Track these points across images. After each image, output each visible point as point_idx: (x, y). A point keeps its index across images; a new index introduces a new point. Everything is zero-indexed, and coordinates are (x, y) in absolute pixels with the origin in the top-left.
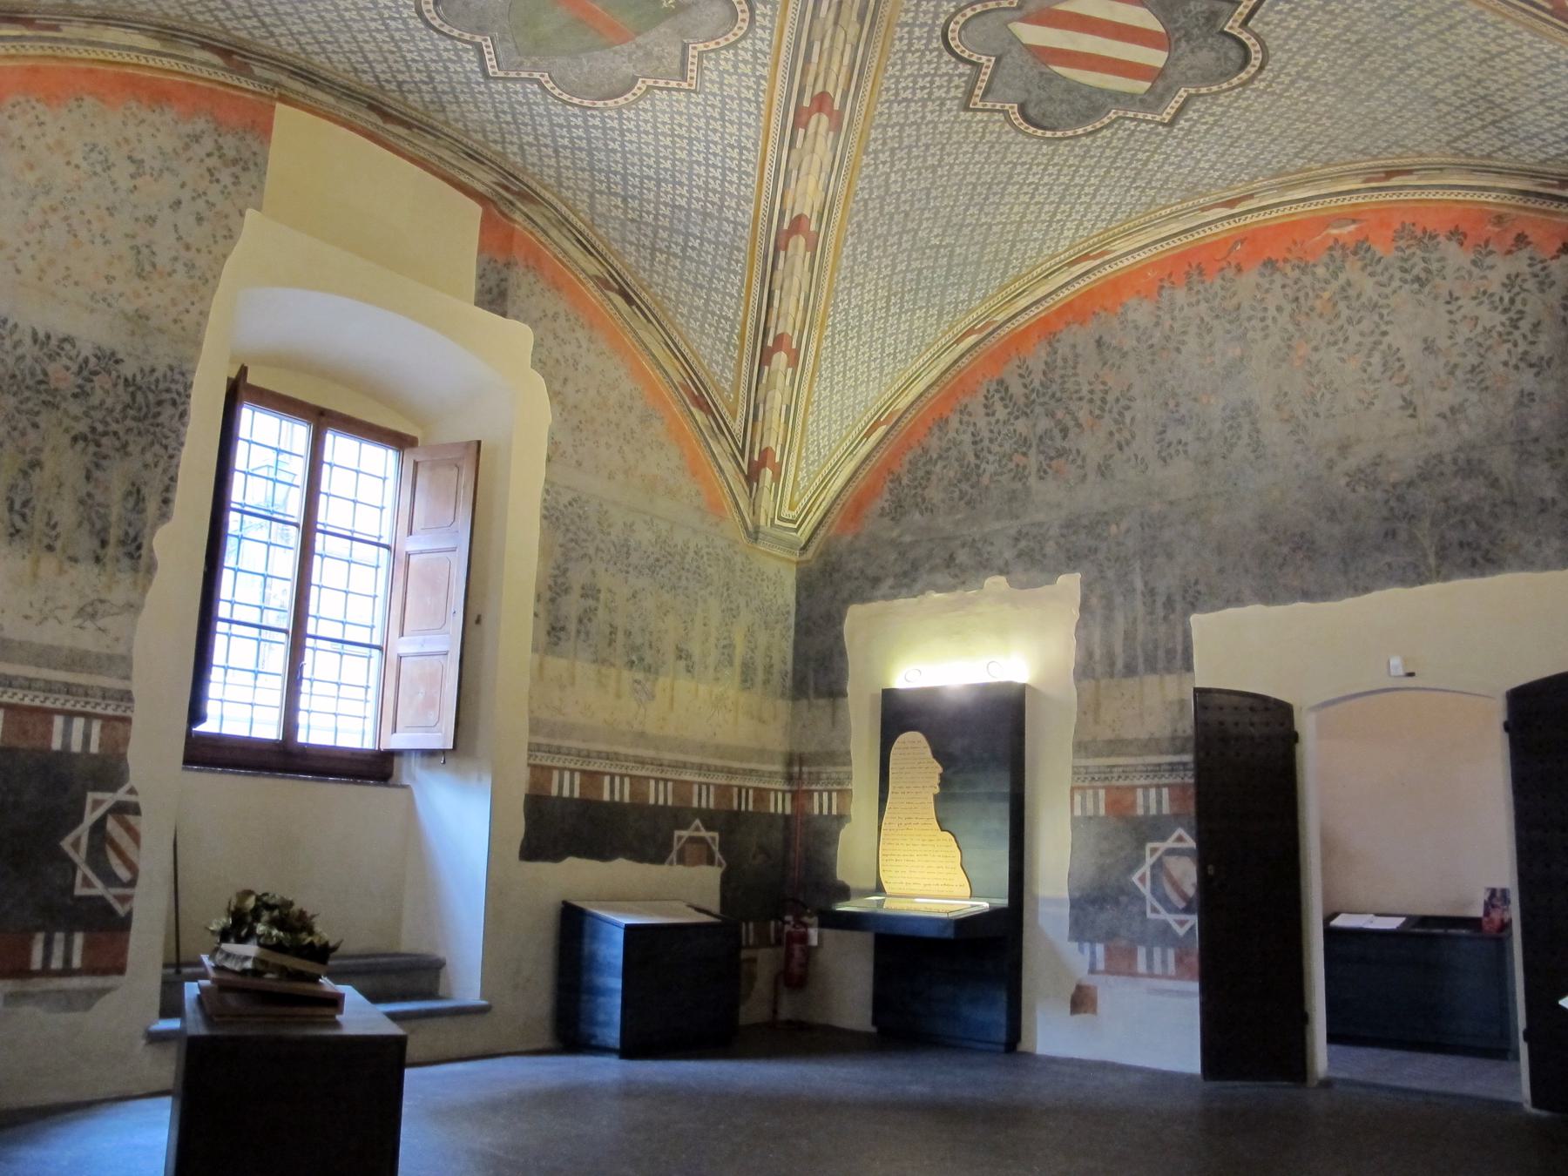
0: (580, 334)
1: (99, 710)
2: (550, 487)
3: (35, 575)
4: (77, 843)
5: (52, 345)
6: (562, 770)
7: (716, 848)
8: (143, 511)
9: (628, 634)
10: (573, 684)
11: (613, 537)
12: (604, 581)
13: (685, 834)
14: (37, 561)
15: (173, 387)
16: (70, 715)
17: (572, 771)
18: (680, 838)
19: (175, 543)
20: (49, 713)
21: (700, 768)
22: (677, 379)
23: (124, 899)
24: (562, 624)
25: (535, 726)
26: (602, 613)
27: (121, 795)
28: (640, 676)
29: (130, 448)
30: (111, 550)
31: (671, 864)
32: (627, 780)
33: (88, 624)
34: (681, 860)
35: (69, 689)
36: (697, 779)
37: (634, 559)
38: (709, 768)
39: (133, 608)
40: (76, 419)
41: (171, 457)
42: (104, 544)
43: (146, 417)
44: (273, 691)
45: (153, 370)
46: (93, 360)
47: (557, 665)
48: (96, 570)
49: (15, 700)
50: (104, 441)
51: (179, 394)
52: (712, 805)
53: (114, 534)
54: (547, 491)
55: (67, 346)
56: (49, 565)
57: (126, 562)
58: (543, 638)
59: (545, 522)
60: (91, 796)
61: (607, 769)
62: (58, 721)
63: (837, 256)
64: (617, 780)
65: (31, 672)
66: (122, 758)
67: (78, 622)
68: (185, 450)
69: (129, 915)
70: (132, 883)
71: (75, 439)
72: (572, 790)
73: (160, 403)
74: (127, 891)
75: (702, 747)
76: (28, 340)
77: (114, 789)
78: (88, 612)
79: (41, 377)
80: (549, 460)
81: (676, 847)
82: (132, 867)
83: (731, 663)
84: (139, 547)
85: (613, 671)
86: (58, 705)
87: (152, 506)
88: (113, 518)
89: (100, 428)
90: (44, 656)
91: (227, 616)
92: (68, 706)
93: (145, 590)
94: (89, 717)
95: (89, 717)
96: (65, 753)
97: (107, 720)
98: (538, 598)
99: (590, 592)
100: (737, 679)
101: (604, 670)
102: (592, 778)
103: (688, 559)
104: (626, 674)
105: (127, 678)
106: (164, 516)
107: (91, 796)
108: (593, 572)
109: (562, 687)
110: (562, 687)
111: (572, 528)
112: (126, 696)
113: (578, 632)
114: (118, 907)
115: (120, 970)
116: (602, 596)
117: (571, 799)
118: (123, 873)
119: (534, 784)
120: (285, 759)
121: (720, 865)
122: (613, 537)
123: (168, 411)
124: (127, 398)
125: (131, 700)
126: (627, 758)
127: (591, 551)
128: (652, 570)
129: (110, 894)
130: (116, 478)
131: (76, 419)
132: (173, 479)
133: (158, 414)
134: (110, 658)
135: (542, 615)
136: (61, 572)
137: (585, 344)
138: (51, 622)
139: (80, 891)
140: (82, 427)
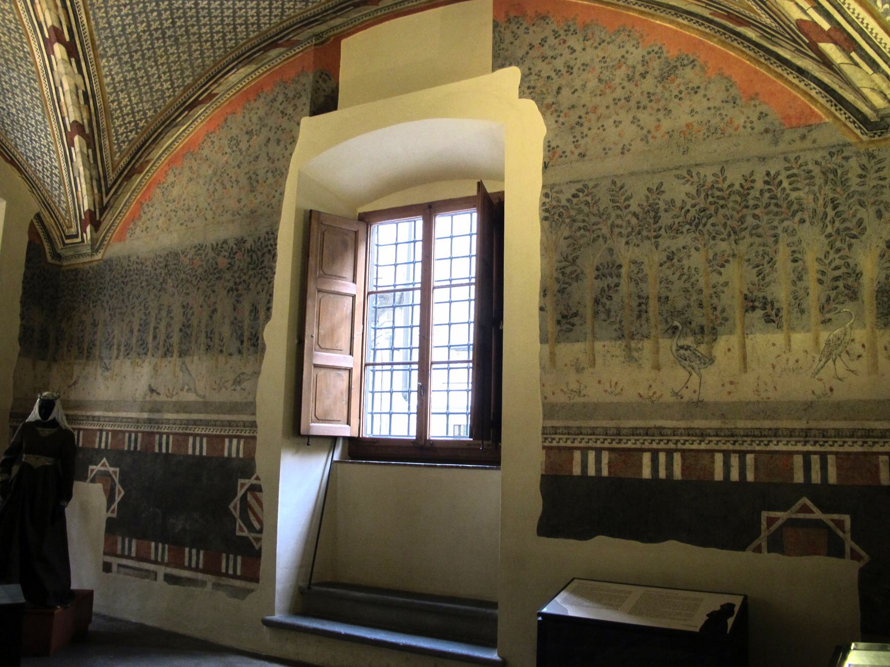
0: (572, 41)
1: (243, 434)
2: (549, 190)
3: (217, 367)
4: (235, 506)
5: (217, 248)
6: (584, 451)
7: (847, 537)
8: (258, 318)
9: (663, 300)
10: (593, 363)
11: (634, 208)
12: (625, 254)
13: (782, 516)
14: (217, 359)
15: (269, 243)
16: (231, 437)
17: (599, 451)
18: (771, 521)
19: (276, 332)
20: (222, 437)
21: (806, 435)
22: (706, 13)
23: (258, 540)
24: (574, 310)
25: (550, 410)
26: (625, 288)
27: (253, 481)
28: (689, 341)
29: (252, 286)
30: (245, 344)
31: (758, 549)
32: (677, 457)
33: (238, 388)
34: (776, 545)
35: (230, 424)
36: (800, 447)
37: (666, 219)
38: (824, 433)
39: (257, 374)
40: (228, 281)
41: (270, 283)
42: (242, 342)
43: (257, 266)
44: (408, 405)
45: (260, 238)
46: (235, 247)
47: (570, 351)
48: (239, 357)
49: (210, 433)
50: (240, 287)
51: (271, 245)
52: (832, 478)
53: (246, 334)
54: (546, 195)
55: (225, 245)
56: (222, 359)
57: (252, 349)
58: (551, 327)
59: (546, 223)
60: (241, 481)
61: (647, 445)
62: (227, 441)
64: (662, 457)
65: (214, 417)
66: (253, 459)
67: (233, 387)
68: (276, 276)
69: (260, 548)
70: (261, 531)
71: (228, 291)
72: (599, 469)
73: (263, 255)
74: (258, 535)
75: (809, 406)
76: (210, 251)
77: (249, 478)
78: (237, 382)
79: (215, 266)
80: (546, 166)
81: (765, 532)
82: (260, 522)
83: (853, 295)
84: (257, 340)
85: (647, 345)
86: (226, 433)
87: (262, 314)
88: (246, 327)
89: (238, 280)
90: (221, 408)
91: (371, 361)
92: (230, 433)
93: (261, 363)
94: (239, 437)
95: (239, 437)
96: (229, 458)
97: (246, 438)
98: (544, 293)
99: (609, 270)
100: (870, 316)
101: (633, 344)
102: (631, 456)
103: (754, 193)
104: (667, 344)
105: (254, 414)
106: (268, 318)
107: (241, 481)
108: (611, 250)
109: (579, 370)
110: (579, 370)
111: (580, 217)
112: (253, 425)
113: (596, 313)
114: (255, 544)
115: (257, 580)
116: (623, 271)
117: (599, 477)
118: (257, 525)
119: (550, 464)
120: (421, 451)
121: (855, 556)
122: (634, 208)
123: (267, 256)
124: (249, 260)
125: (256, 427)
126: (675, 431)
127: (605, 231)
128: (696, 224)
129: (251, 536)
130: (246, 306)
131: (228, 281)
132: (271, 295)
133: (263, 261)
134: (246, 404)
135: (549, 308)
136: (227, 362)
137: (578, 47)
138: (224, 389)
139: (238, 533)
140: (231, 284)
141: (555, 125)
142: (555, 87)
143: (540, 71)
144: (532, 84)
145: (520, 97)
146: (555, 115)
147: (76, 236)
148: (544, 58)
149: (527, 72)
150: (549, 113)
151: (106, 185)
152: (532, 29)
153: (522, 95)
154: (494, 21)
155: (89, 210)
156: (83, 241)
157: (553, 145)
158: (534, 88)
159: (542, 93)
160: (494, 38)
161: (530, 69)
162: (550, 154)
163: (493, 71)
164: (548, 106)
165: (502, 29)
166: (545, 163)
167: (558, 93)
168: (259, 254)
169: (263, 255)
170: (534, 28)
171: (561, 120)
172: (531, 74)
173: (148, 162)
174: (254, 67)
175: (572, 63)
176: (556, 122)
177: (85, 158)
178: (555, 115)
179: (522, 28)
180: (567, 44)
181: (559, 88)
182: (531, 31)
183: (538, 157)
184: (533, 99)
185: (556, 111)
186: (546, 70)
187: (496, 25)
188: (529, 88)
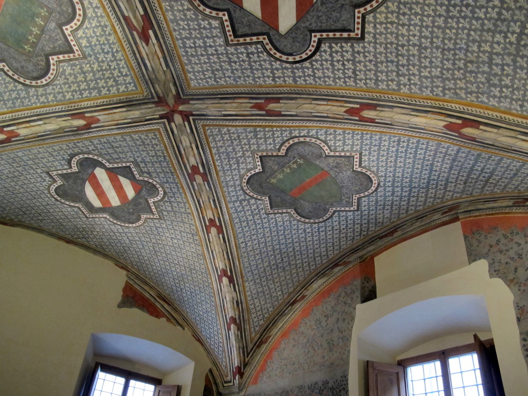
0: (517, 239)
63: (494, 109)
73: (340, 391)
80: (519, 320)
123: (343, 392)
141: (519, 292)
142: (513, 269)
143: (500, 260)
144: (497, 268)
145: (491, 278)
146: (517, 285)
147: (230, 382)
148: (501, 252)
149: (492, 262)
150: (512, 285)
151: (247, 351)
152: (489, 236)
153: (491, 276)
154: (464, 235)
155: (238, 366)
156: (234, 384)
157: (521, 305)
158: (499, 271)
159: (505, 273)
160: (466, 244)
161: (493, 260)
162: (520, 311)
163: (470, 264)
164: (512, 281)
165: (470, 239)
166: (518, 318)
167: (516, 272)
168: (338, 390)
169: (340, 391)
170: (490, 235)
171: (522, 288)
172: (494, 262)
173: (270, 337)
174: (326, 278)
175: (520, 252)
176: (519, 290)
177: (237, 336)
178: (517, 285)
179: (483, 236)
180: (514, 241)
181: (516, 269)
182: (488, 237)
183: (512, 314)
184: (500, 277)
185: (517, 283)
186: (504, 259)
187: (466, 237)
188: (495, 271)
